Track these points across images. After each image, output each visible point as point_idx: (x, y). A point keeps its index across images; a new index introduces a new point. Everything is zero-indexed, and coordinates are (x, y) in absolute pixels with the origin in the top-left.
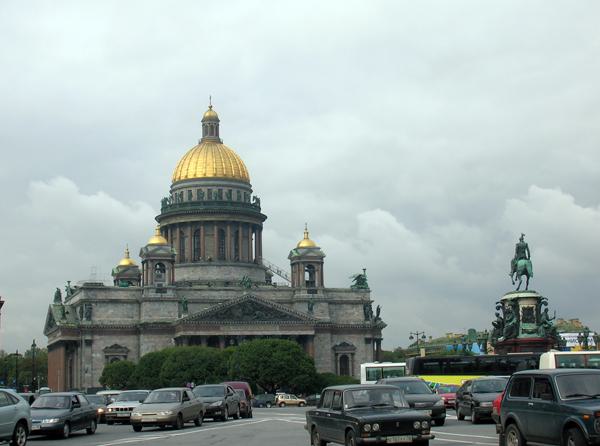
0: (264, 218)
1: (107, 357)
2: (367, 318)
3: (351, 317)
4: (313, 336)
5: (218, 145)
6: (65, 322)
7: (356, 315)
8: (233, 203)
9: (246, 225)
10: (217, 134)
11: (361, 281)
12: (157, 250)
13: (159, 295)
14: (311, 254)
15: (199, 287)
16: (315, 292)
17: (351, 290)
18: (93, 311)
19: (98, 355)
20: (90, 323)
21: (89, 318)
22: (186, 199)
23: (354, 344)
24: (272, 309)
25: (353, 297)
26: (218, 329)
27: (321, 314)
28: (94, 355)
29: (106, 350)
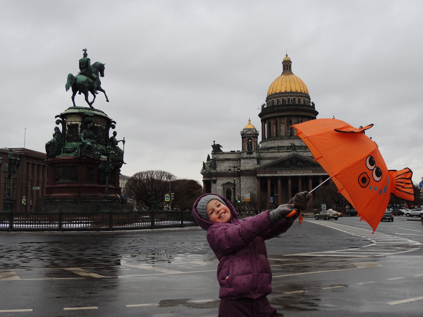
1: (224, 188)
5: (290, 76)
6: (205, 171)
10: (290, 70)
12: (247, 132)
13: (248, 156)
15: (272, 151)
18: (217, 165)
19: (220, 188)
20: (215, 171)
21: (215, 168)
22: (276, 103)
24: (307, 161)
26: (277, 173)
28: (217, 188)
29: (223, 185)
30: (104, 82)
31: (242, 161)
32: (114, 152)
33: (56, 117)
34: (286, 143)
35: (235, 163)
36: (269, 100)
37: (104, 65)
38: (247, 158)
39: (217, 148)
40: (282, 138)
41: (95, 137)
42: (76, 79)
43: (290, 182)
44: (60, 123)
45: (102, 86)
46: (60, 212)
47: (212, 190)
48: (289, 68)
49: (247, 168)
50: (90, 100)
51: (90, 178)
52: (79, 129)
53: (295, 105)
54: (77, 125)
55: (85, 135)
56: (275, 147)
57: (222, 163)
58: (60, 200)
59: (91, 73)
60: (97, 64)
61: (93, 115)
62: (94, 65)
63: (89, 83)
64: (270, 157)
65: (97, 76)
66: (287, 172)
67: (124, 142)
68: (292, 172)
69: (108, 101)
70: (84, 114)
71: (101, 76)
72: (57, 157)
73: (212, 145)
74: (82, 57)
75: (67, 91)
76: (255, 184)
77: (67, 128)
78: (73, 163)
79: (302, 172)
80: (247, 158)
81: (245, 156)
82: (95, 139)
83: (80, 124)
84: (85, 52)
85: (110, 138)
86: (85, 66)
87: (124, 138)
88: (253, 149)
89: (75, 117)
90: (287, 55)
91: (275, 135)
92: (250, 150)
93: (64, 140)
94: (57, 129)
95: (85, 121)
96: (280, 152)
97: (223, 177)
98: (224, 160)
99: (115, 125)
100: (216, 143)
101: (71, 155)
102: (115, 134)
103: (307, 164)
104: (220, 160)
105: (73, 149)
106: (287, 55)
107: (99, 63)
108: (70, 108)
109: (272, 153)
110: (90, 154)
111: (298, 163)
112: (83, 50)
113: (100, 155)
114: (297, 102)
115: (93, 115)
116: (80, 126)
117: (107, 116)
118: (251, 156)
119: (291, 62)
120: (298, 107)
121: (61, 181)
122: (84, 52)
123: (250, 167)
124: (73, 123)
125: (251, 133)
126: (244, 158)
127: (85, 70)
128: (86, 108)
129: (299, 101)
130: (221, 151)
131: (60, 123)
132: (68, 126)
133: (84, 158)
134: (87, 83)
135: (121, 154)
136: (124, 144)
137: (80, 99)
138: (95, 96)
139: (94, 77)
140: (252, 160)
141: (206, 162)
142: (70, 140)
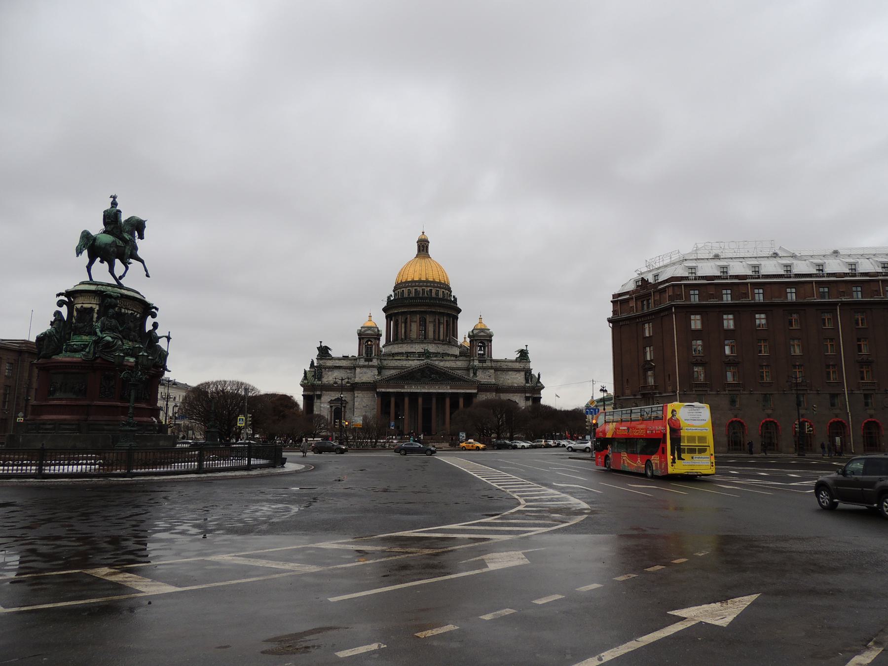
0: (459, 311)
1: (331, 407)
2: (527, 381)
3: (515, 381)
4: (476, 394)
6: (306, 382)
7: (518, 379)
8: (440, 299)
9: (448, 315)
10: (427, 251)
11: (524, 355)
12: (365, 331)
13: (367, 363)
14: (482, 334)
15: (399, 358)
16: (485, 361)
17: (516, 361)
18: (323, 374)
19: (325, 405)
20: (320, 382)
21: (320, 379)
22: (406, 295)
23: (517, 401)
25: (517, 365)
26: (404, 388)
27: (483, 377)
28: (322, 405)
29: (331, 402)
30: (143, 247)
31: (358, 370)
32: (146, 354)
33: (58, 295)
34: (418, 348)
35: (348, 373)
36: (397, 290)
37: (145, 221)
38: (364, 366)
39: (324, 352)
40: (412, 342)
41: (121, 329)
42: (95, 239)
43: (420, 400)
44: (64, 306)
45: (140, 253)
46: (42, 447)
47: (315, 409)
48: (425, 249)
49: (364, 379)
50: (118, 273)
51: (106, 393)
52: (95, 316)
53: (431, 298)
54: (92, 309)
55: (103, 324)
56: (403, 353)
57: (330, 373)
58: (53, 426)
59: (121, 232)
60: (134, 220)
61: (120, 295)
62: (126, 221)
63: (117, 246)
64: (396, 365)
65: (131, 237)
66: (418, 387)
67: (169, 338)
68: (424, 388)
69: (147, 276)
70: (105, 293)
71: (139, 238)
72: (54, 357)
73: (317, 348)
74: (109, 206)
75: (78, 256)
76: (374, 402)
77: (75, 313)
78: (80, 367)
79: (437, 388)
80: (364, 366)
81: (362, 364)
82: (120, 332)
83: (97, 308)
84: (114, 200)
85: (147, 331)
86: (112, 221)
87: (169, 332)
88: (373, 355)
89: (89, 297)
90: (423, 233)
91: (403, 337)
92: (369, 355)
93: (68, 332)
94: (58, 314)
95: (105, 305)
96: (409, 360)
97: (331, 391)
98: (333, 368)
99: (156, 312)
100: (323, 345)
101: (78, 357)
102: (155, 325)
103: (444, 377)
104: (327, 368)
105: (82, 346)
106: (423, 233)
107: (136, 218)
108: (83, 283)
109: (398, 361)
110: (109, 355)
111: (432, 376)
112: (111, 197)
113: (124, 357)
114: (434, 295)
115: (120, 295)
116: (96, 311)
117: (145, 298)
118: (370, 363)
119: (429, 242)
120: (435, 302)
121: (58, 395)
122: (112, 199)
123: (369, 378)
124: (85, 306)
125: (372, 332)
126: (360, 367)
127: (112, 226)
128: (109, 285)
129: (437, 294)
130: (330, 355)
131: (64, 306)
132: (77, 310)
133: (98, 361)
134: (112, 247)
135: (163, 355)
136: (168, 341)
137: (101, 272)
138: (127, 268)
139: (126, 239)
140: (371, 369)
141: (309, 369)
142: (78, 332)
